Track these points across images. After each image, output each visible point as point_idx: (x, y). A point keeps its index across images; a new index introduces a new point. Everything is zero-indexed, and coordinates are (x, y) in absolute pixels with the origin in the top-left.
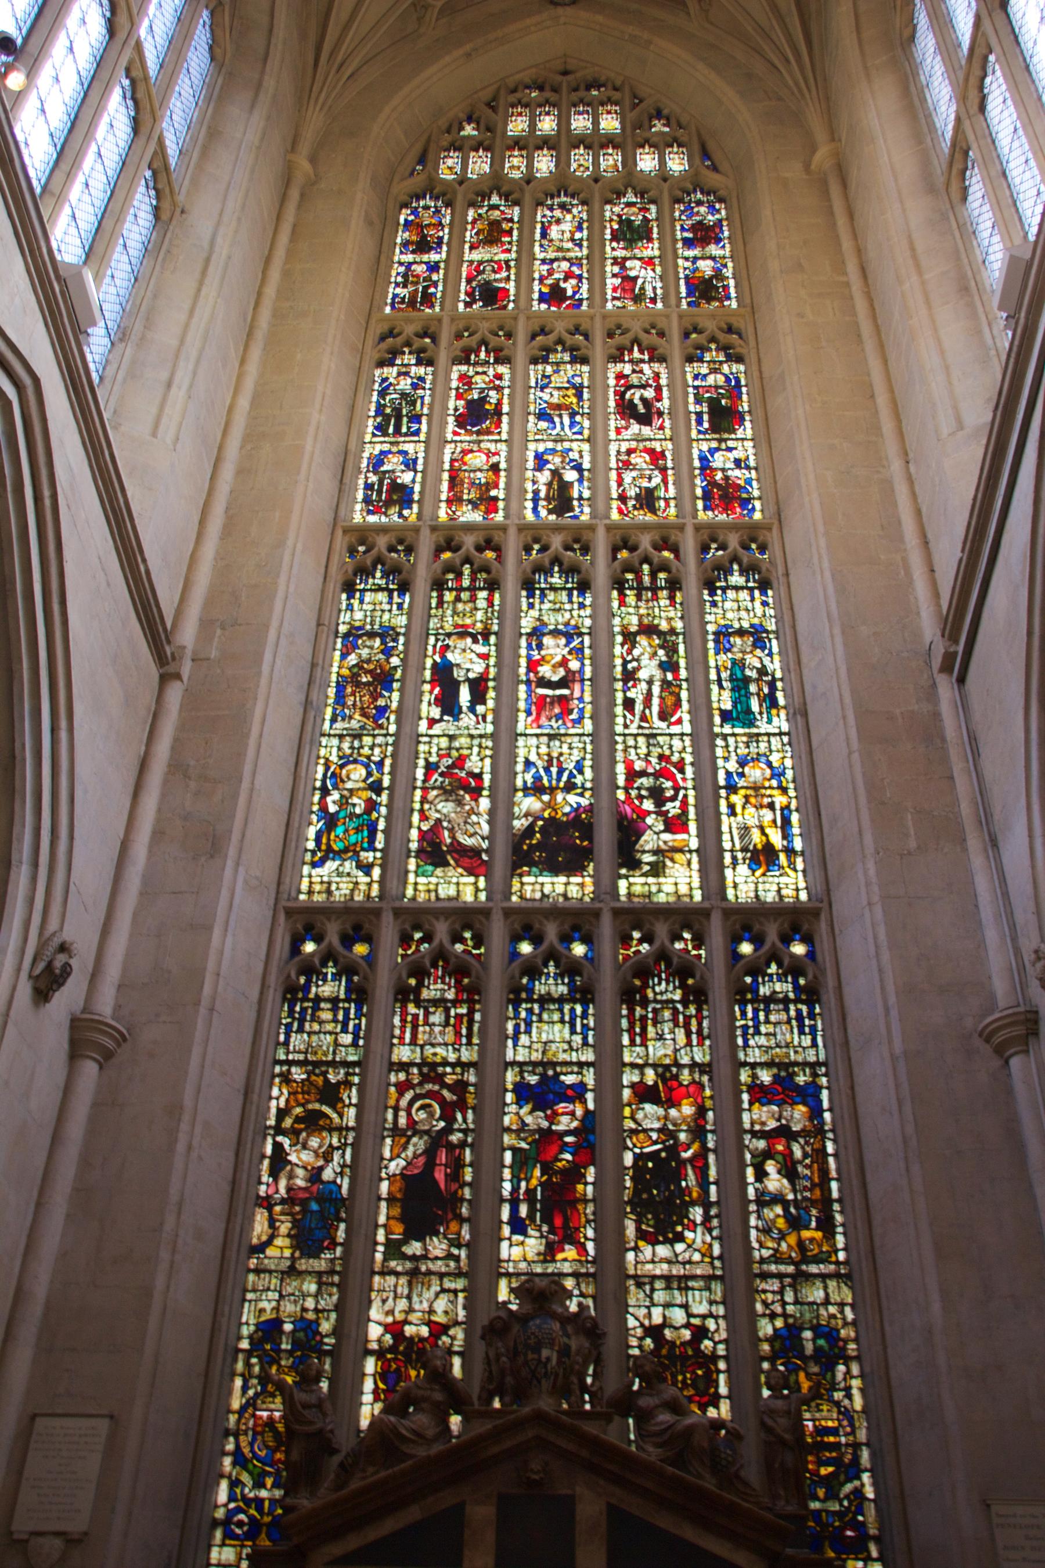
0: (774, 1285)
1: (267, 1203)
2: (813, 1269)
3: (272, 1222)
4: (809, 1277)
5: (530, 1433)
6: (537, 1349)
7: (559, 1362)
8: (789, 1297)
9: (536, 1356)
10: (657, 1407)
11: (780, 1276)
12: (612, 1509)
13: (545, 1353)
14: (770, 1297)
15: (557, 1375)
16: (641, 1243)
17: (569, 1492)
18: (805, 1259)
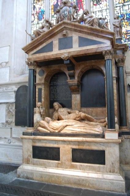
0: (119, 8)
1: (33, 15)
2: (126, 4)
3: (34, 17)
4: (125, 5)
5: (63, 26)
6: (64, 12)
7: (68, 14)
8: (121, 9)
9: (64, 13)
10: (88, 18)
11: (120, 6)
12: (79, 37)
13: (66, 12)
14: (117, 10)
15: (68, 16)
16: (94, 6)
17: (71, 36)
18: (124, 2)
